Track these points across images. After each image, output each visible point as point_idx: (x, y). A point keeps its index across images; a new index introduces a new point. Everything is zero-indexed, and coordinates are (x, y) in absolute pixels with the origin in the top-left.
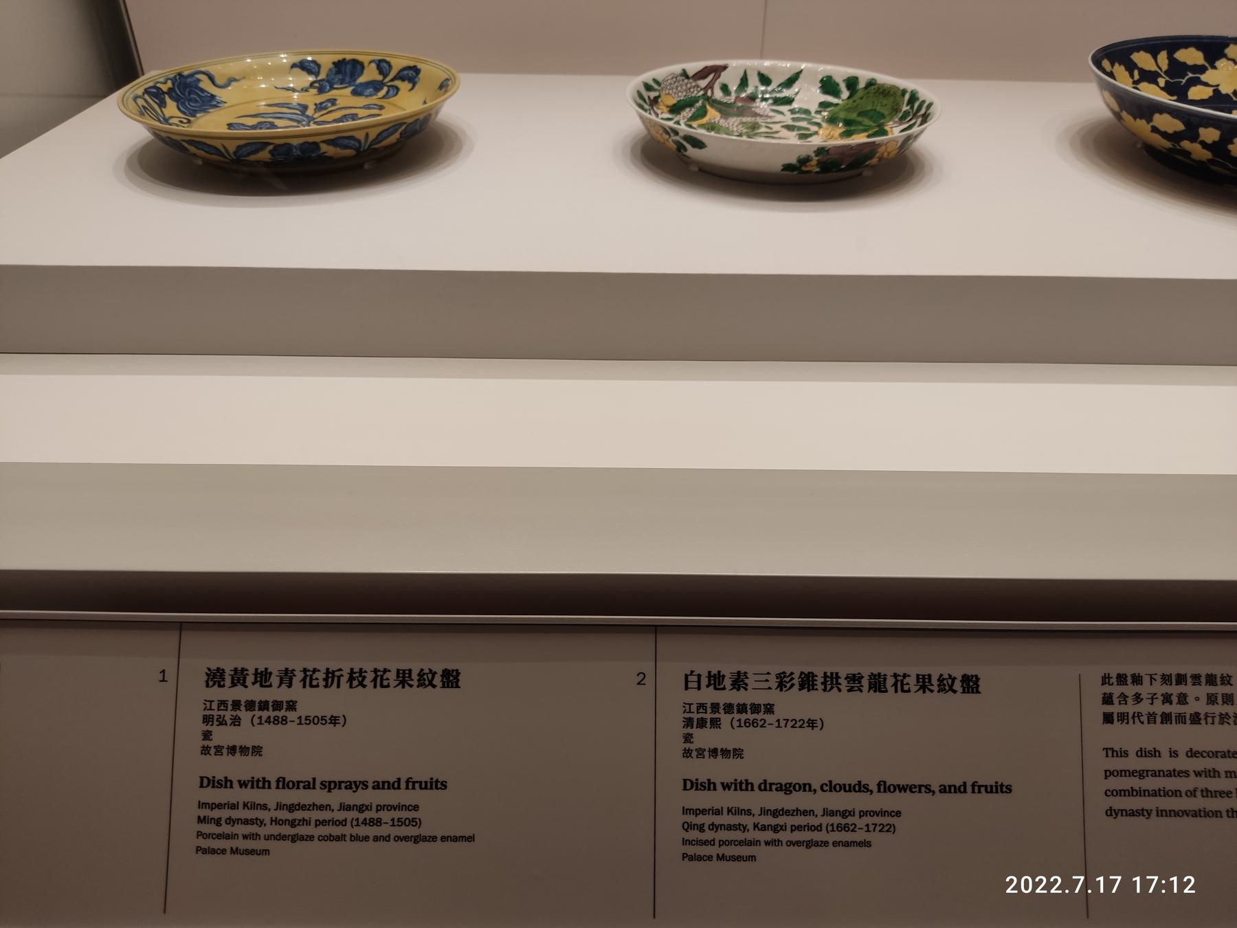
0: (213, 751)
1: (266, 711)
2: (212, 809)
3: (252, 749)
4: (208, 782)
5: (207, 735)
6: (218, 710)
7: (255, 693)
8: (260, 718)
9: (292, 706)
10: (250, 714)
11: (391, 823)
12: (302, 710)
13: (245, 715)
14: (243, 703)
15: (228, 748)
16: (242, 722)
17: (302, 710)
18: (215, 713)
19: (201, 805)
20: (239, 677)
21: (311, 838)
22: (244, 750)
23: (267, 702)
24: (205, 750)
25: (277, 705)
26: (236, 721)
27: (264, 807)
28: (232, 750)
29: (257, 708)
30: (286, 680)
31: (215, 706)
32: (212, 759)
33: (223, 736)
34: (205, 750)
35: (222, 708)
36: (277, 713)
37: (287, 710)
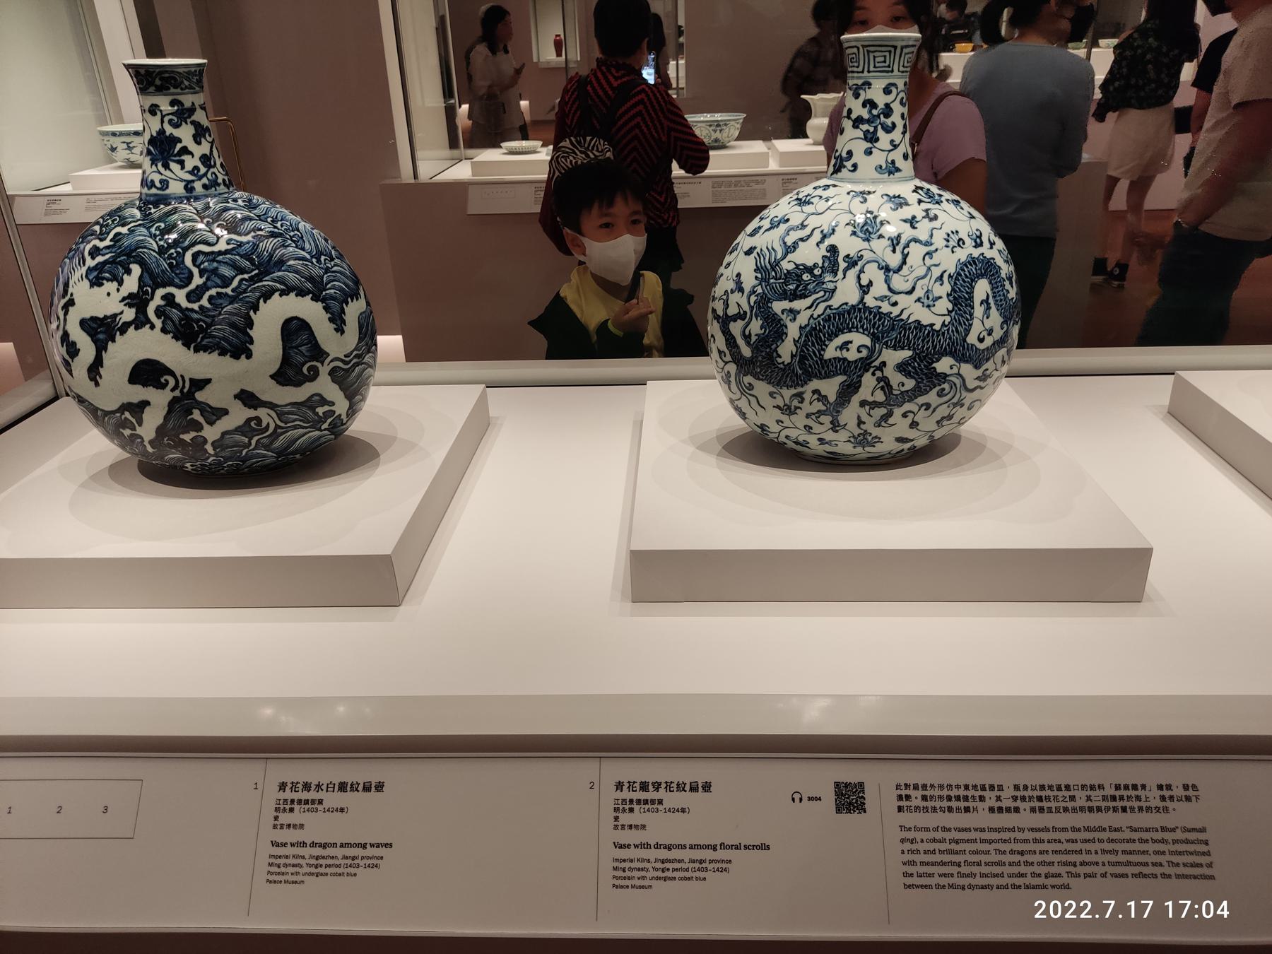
5: (276, 818)
7: (304, 796)
9: (321, 802)
10: (299, 806)
11: (364, 866)
12: (326, 805)
13: (296, 807)
16: (295, 812)
17: (326, 805)
18: (282, 807)
20: (294, 787)
21: (326, 874)
22: (295, 826)
23: (308, 800)
25: (313, 802)
26: (292, 810)
31: (281, 802)
32: (278, 831)
33: (285, 818)
34: (275, 827)
36: (313, 806)
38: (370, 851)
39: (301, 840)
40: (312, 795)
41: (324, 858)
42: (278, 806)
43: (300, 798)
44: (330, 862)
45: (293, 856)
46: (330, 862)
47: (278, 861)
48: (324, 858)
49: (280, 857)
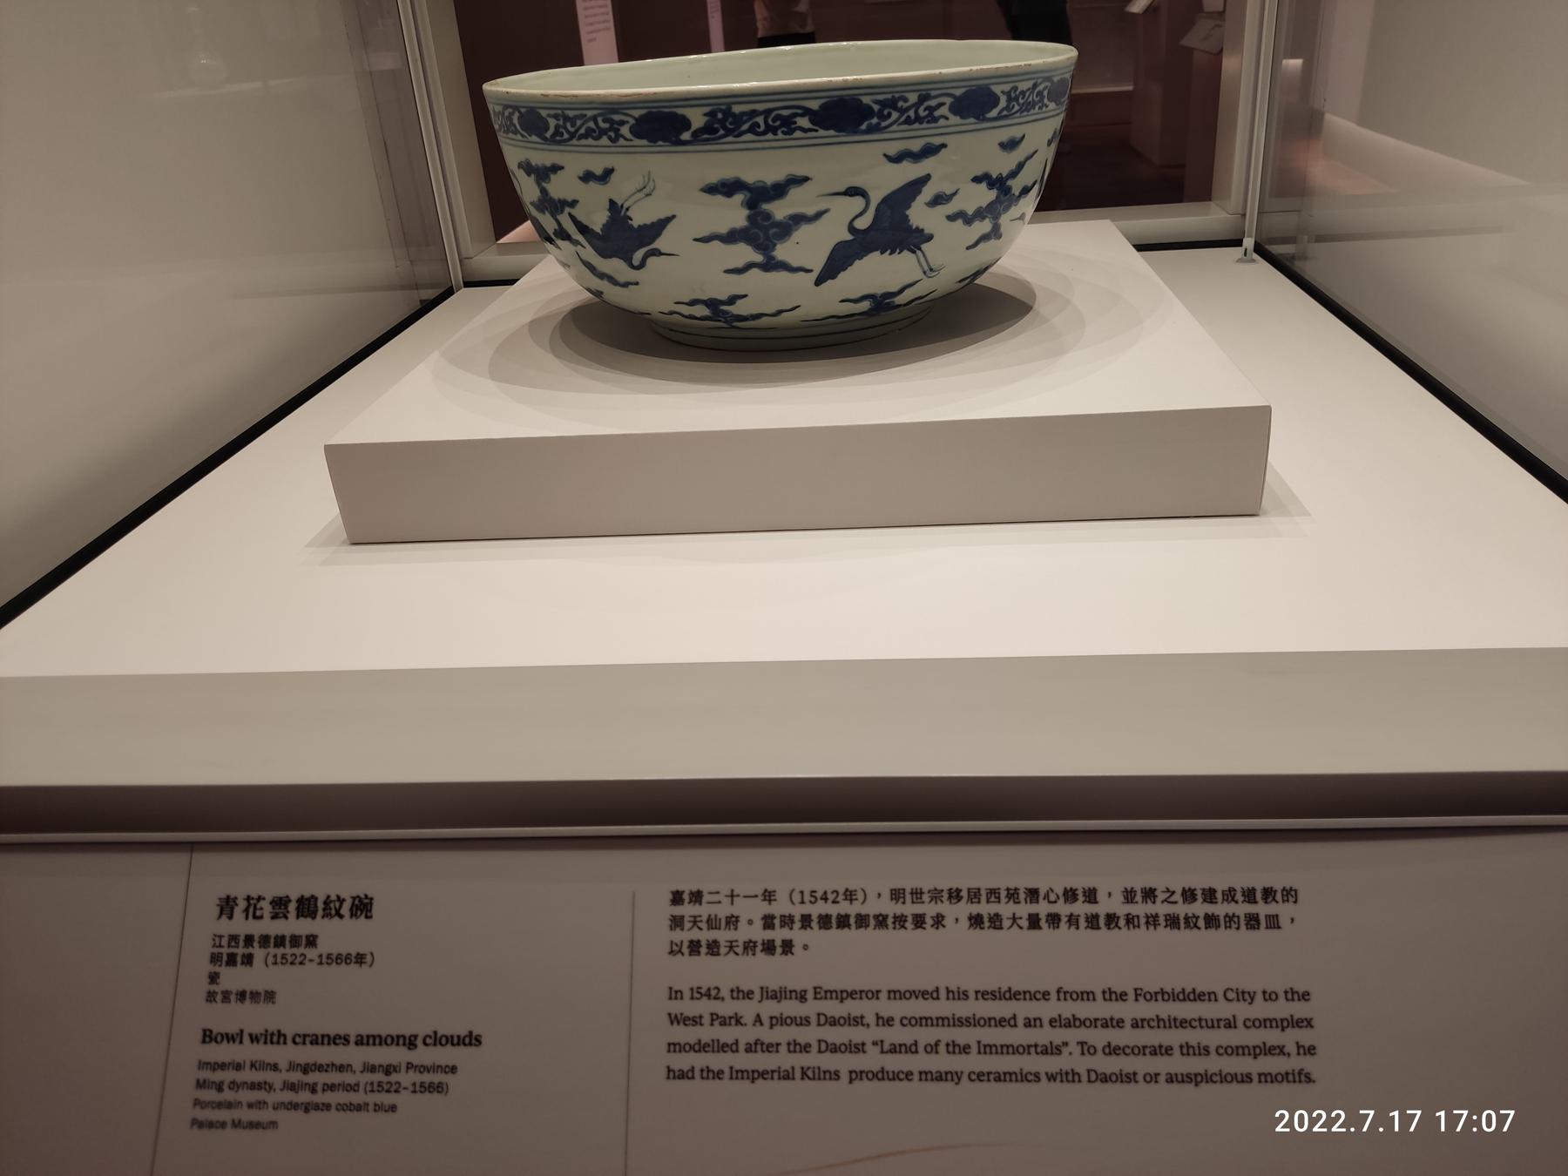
0: (219, 997)
1: (282, 949)
2: (214, 1070)
3: (265, 995)
4: (208, 1036)
5: (214, 978)
6: (229, 947)
8: (275, 956)
9: (312, 941)
13: (258, 953)
14: (256, 938)
15: (237, 994)
19: (203, 1065)
20: (252, 907)
22: (255, 996)
23: (283, 937)
24: (211, 997)
25: (295, 940)
26: (248, 960)
27: (275, 1067)
28: (242, 996)
29: (272, 945)
30: (227, 910)
31: (225, 942)
32: (218, 1006)
33: (233, 978)
35: (233, 944)
36: (295, 950)
37: (306, 946)
38: (424, 1055)
39: (272, 1028)
40: (294, 926)
41: (320, 1068)
42: (216, 950)
43: (264, 933)
44: (334, 1077)
45: (253, 1065)
46: (334, 1077)
47: (218, 1076)
48: (320, 1068)
49: (223, 1066)
